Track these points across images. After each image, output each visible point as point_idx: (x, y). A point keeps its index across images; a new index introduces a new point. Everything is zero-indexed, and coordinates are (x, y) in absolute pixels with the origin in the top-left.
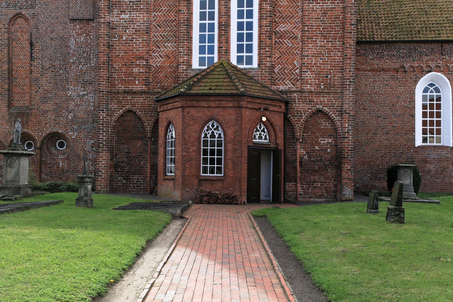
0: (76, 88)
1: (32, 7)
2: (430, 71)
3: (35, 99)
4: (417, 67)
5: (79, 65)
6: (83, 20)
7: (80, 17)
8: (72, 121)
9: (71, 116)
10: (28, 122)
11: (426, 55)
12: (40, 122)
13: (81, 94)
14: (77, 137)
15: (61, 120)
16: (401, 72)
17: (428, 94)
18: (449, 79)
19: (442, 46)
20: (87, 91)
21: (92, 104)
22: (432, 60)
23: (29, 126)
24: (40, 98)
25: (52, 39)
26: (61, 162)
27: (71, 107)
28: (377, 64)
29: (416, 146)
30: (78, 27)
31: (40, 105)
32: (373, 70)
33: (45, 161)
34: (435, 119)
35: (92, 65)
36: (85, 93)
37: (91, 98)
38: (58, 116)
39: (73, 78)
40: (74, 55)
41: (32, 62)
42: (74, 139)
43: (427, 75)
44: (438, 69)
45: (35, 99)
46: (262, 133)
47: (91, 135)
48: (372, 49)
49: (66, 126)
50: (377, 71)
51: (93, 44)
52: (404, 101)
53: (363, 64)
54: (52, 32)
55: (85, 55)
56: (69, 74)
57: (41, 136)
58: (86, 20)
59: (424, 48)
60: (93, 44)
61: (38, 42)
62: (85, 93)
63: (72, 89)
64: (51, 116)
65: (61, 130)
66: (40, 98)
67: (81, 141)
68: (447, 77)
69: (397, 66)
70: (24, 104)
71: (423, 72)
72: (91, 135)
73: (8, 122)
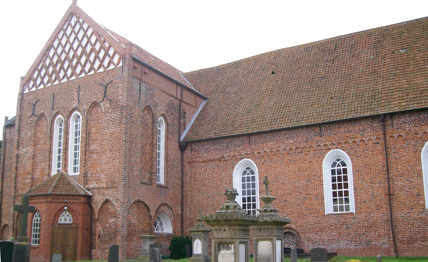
2: (243, 158)
4: (233, 156)
11: (239, 146)
16: (223, 161)
17: (246, 176)
18: (256, 163)
19: (250, 138)
22: (243, 149)
28: (207, 156)
32: (204, 161)
34: (251, 196)
43: (241, 162)
44: (247, 156)
46: (67, 217)
48: (203, 146)
50: (207, 162)
52: (226, 183)
53: (197, 157)
59: (237, 141)
68: (254, 161)
69: (220, 156)
71: (236, 159)
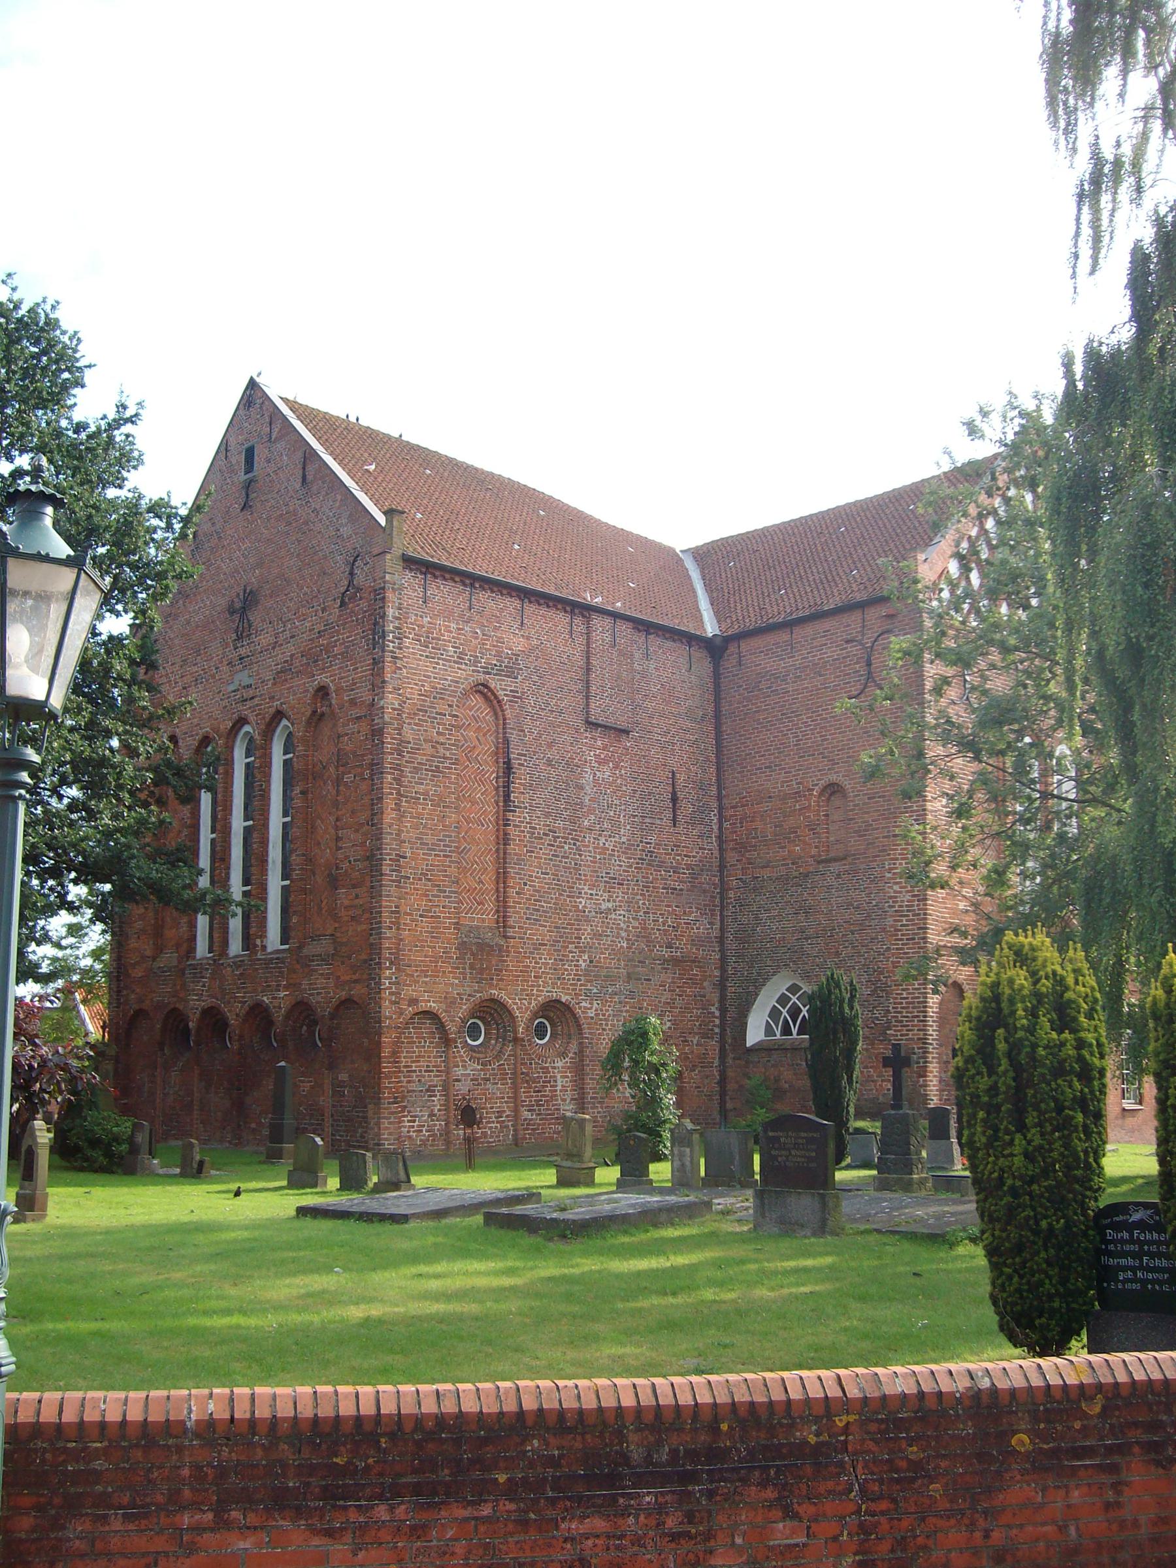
0: (594, 892)
1: (511, 673)
3: (517, 913)
5: (600, 835)
6: (611, 728)
7: (611, 722)
8: (587, 973)
9: (585, 961)
10: (501, 971)
12: (526, 970)
13: (603, 907)
14: (597, 1015)
15: (566, 970)
20: (614, 901)
21: (624, 934)
23: (502, 980)
24: (528, 909)
25: (549, 763)
26: (559, 1076)
27: (585, 938)
29: (749, 1043)
30: (599, 743)
31: (527, 929)
33: (527, 1074)
35: (624, 839)
36: (610, 905)
37: (620, 917)
38: (561, 960)
39: (589, 866)
40: (591, 811)
41: (510, 815)
42: (592, 1018)
45: (517, 913)
47: (627, 1011)
49: (575, 985)
51: (624, 788)
54: (550, 745)
55: (612, 813)
56: (580, 855)
57: (527, 1009)
58: (615, 729)
60: (624, 788)
61: (522, 765)
62: (610, 905)
63: (586, 893)
64: (546, 958)
65: (566, 994)
66: (528, 909)
67: (607, 1025)
70: (483, 920)
72: (627, 1011)
73: (458, 968)
